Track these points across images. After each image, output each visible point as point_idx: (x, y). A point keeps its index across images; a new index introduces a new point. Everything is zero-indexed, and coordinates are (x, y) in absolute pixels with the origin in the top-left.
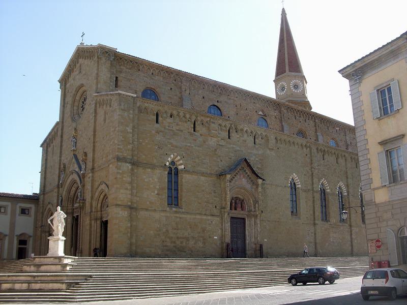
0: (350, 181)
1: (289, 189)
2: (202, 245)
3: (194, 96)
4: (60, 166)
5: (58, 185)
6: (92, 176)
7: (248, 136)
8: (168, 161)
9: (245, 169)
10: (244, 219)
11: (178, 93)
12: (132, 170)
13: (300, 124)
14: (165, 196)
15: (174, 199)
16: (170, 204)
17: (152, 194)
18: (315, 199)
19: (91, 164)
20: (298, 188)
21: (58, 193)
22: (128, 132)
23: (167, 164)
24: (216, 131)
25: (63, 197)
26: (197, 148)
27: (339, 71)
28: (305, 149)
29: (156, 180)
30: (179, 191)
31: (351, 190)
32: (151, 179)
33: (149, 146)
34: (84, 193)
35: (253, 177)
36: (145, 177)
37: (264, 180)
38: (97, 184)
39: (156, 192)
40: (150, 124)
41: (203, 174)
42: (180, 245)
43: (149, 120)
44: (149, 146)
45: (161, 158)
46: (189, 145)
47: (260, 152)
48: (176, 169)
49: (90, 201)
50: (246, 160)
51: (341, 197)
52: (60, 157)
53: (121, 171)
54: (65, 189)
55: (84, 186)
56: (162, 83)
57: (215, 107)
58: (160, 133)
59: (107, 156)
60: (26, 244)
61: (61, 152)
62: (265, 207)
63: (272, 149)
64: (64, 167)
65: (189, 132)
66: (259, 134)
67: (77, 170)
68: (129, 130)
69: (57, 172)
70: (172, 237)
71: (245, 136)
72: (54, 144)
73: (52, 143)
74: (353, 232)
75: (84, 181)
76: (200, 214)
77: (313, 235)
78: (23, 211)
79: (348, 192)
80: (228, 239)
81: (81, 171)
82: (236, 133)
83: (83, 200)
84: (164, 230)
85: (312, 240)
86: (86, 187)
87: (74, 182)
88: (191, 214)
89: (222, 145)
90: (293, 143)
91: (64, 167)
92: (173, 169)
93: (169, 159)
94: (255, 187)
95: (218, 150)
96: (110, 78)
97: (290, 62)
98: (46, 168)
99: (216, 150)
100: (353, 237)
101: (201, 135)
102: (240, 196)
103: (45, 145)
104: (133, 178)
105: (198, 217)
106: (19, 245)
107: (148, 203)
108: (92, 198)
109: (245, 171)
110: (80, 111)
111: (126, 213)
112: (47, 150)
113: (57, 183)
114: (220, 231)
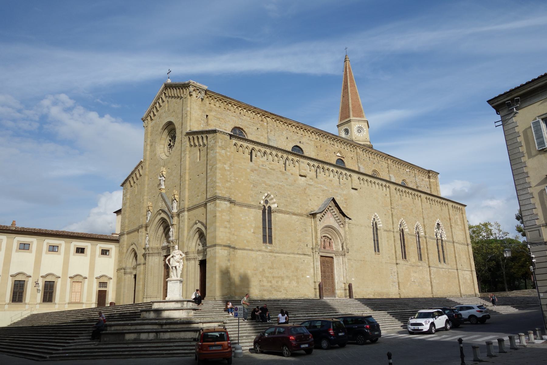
0: (426, 221)
1: (372, 230)
2: (296, 285)
3: (279, 136)
10: (332, 257)
11: (264, 133)
12: (230, 208)
13: (374, 165)
14: (261, 236)
15: (268, 238)
16: (265, 241)
17: (249, 232)
18: (396, 238)
22: (226, 170)
23: (262, 202)
24: (305, 170)
26: (288, 187)
27: (489, 102)
30: (273, 230)
31: (427, 230)
33: (245, 184)
36: (241, 215)
37: (350, 219)
39: (252, 231)
40: (245, 163)
42: (276, 284)
43: (244, 159)
44: (245, 184)
45: (256, 196)
46: (281, 184)
47: (345, 192)
48: (270, 207)
50: (334, 200)
51: (419, 236)
53: (220, 209)
56: (249, 123)
57: (298, 148)
58: (255, 172)
60: (106, 287)
62: (351, 246)
65: (281, 171)
68: (227, 167)
70: (268, 277)
71: (332, 175)
74: (432, 271)
76: (293, 253)
77: (396, 274)
78: (104, 252)
79: (425, 232)
80: (319, 280)
82: (323, 173)
84: (261, 269)
85: (396, 280)
88: (285, 253)
92: (267, 207)
93: (264, 198)
95: (307, 190)
96: (201, 115)
97: (354, 107)
100: (432, 276)
101: (292, 174)
102: (327, 235)
104: (231, 216)
105: (292, 256)
106: (100, 287)
107: (245, 241)
110: (166, 149)
111: (226, 252)
114: (312, 270)
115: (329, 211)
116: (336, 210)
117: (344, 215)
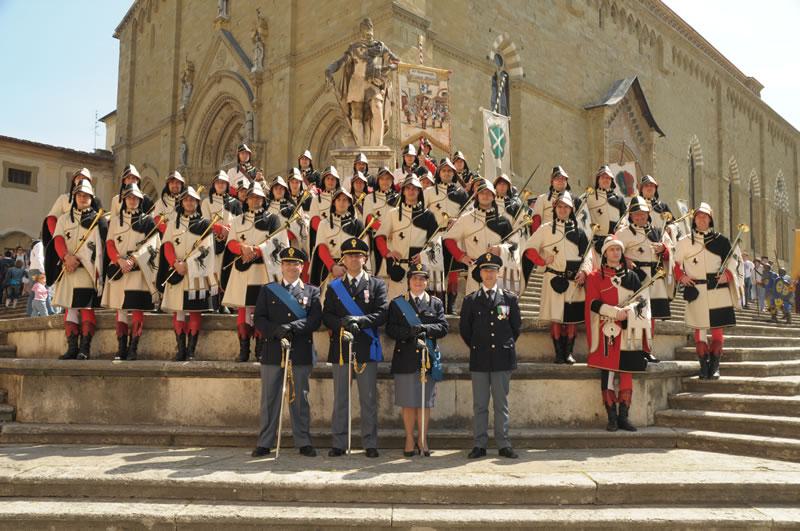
4: (176, 70)
5: (174, 116)
6: (292, 75)
7: (630, 30)
8: (493, 50)
9: (630, 103)
19: (288, 41)
20: (699, 167)
21: (173, 135)
23: (492, 56)
25: (190, 140)
28: (710, 87)
29: (470, 92)
32: (459, 87)
34: (260, 124)
35: (643, 123)
37: (663, 135)
38: (307, 94)
41: (558, 101)
46: (532, 20)
49: (285, 139)
52: (177, 47)
54: (197, 122)
55: (260, 105)
59: (347, 12)
61: (178, 36)
63: (667, 73)
64: (192, 70)
66: (650, 31)
67: (235, 69)
69: (171, 84)
71: (626, 29)
72: (152, 22)
73: (149, 21)
75: (259, 92)
81: (251, 65)
83: (259, 141)
86: (266, 109)
87: (225, 102)
89: (589, 40)
90: (697, 71)
91: (192, 70)
93: (496, 45)
94: (642, 149)
98: (132, 83)
99: (579, 47)
103: (129, 29)
108: (292, 132)
109: (629, 109)
112: (134, 41)
113: (168, 112)
115: (621, 112)
116: (636, 110)
117: (652, 124)
